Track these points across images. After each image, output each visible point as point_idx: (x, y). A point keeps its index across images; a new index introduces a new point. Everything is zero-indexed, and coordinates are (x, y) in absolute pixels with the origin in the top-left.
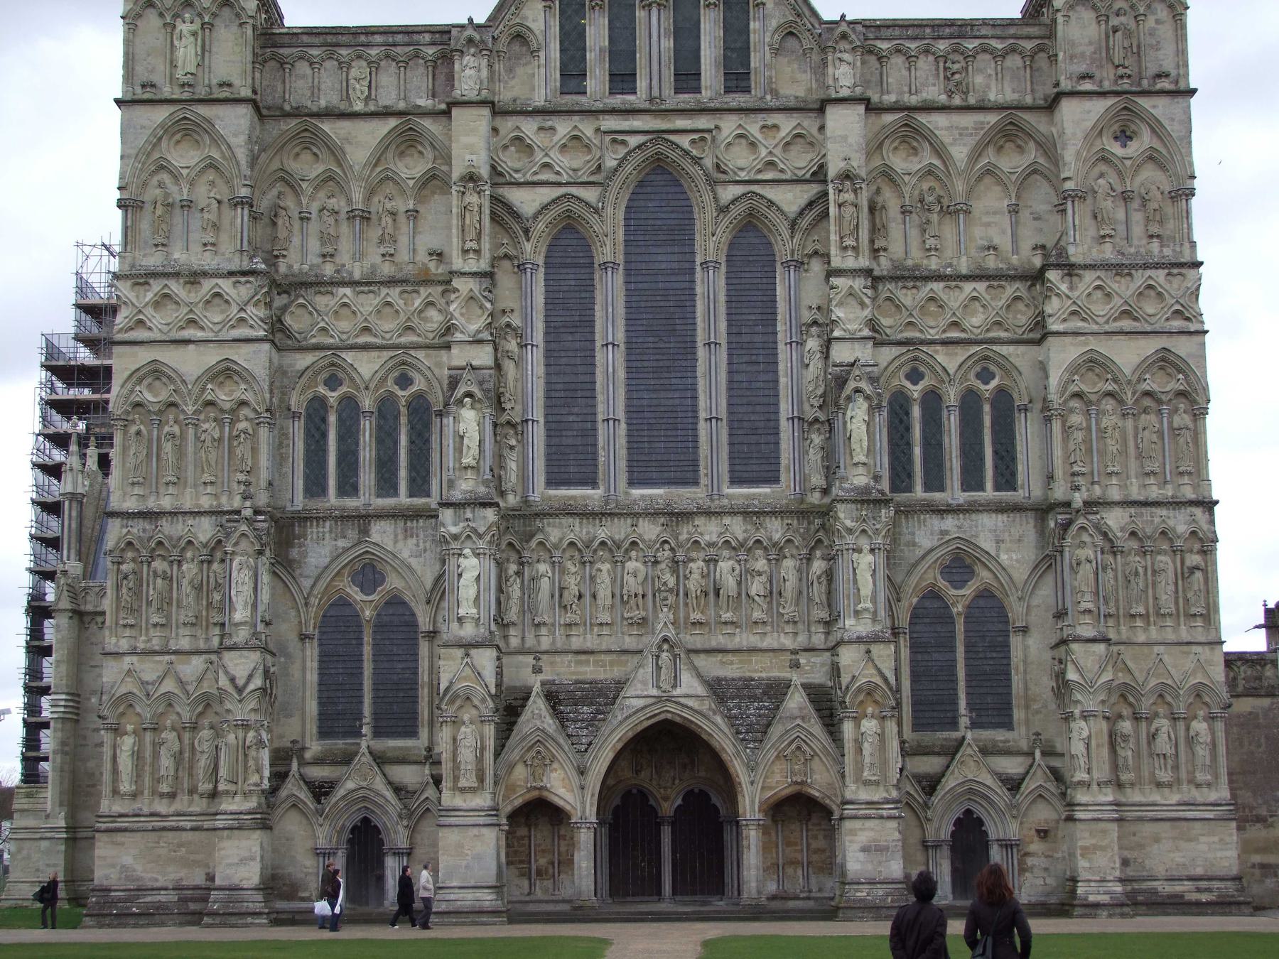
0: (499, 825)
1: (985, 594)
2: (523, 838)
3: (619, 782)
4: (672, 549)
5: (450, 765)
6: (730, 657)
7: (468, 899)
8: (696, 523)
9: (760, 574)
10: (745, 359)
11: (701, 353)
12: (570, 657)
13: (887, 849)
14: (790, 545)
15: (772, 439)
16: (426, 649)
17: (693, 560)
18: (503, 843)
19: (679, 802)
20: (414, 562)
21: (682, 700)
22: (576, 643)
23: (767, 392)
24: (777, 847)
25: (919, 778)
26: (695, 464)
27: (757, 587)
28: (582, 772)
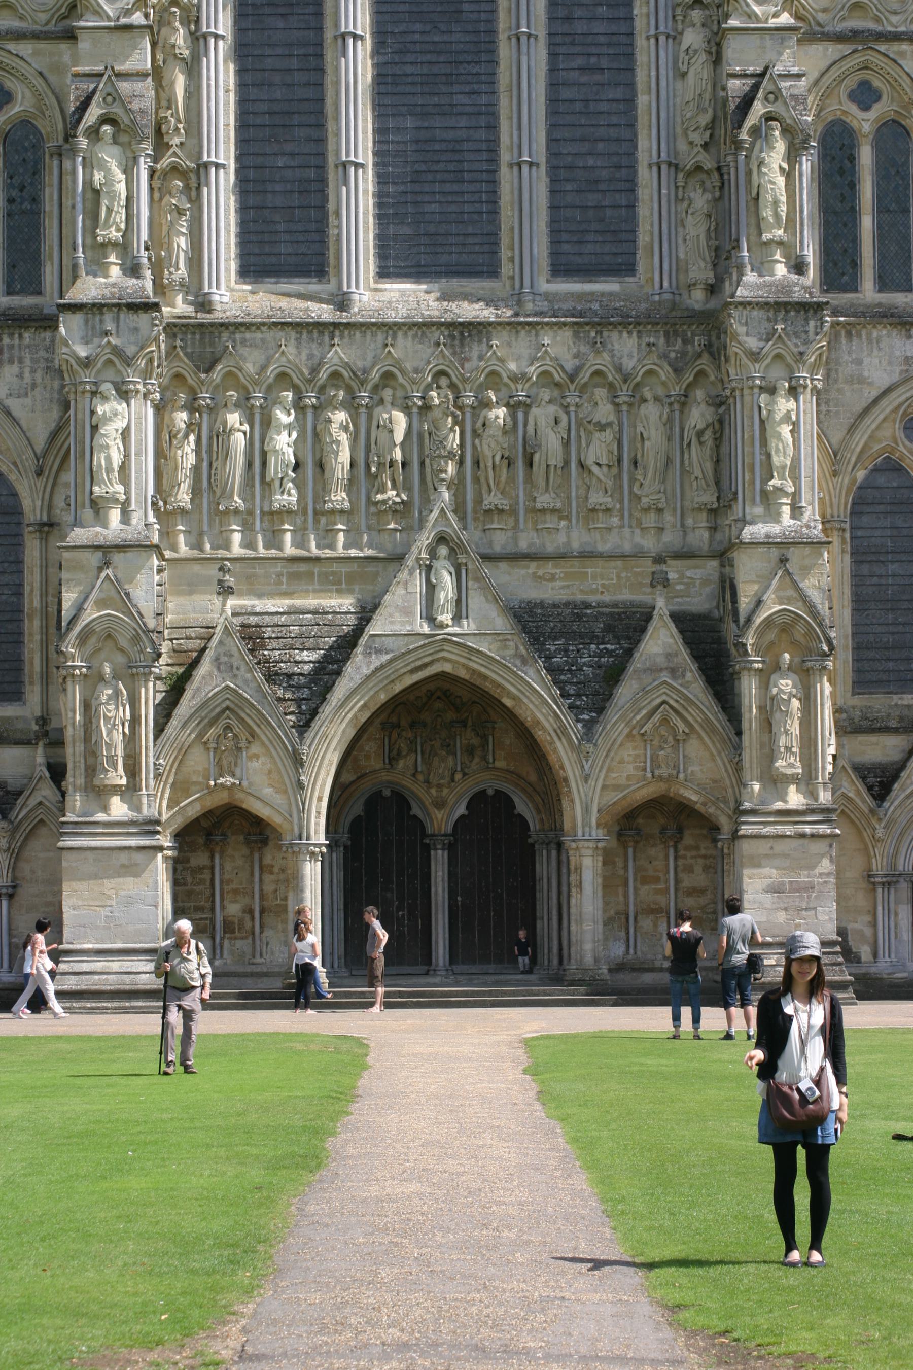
2: (201, 869)
4: (452, 386)
5: (80, 748)
6: (549, 568)
9: (602, 427)
10: (580, 61)
11: (505, 51)
15: (622, 200)
16: (37, 554)
19: (461, 810)
23: (614, 119)
24: (626, 885)
25: (863, 771)
26: (492, 241)
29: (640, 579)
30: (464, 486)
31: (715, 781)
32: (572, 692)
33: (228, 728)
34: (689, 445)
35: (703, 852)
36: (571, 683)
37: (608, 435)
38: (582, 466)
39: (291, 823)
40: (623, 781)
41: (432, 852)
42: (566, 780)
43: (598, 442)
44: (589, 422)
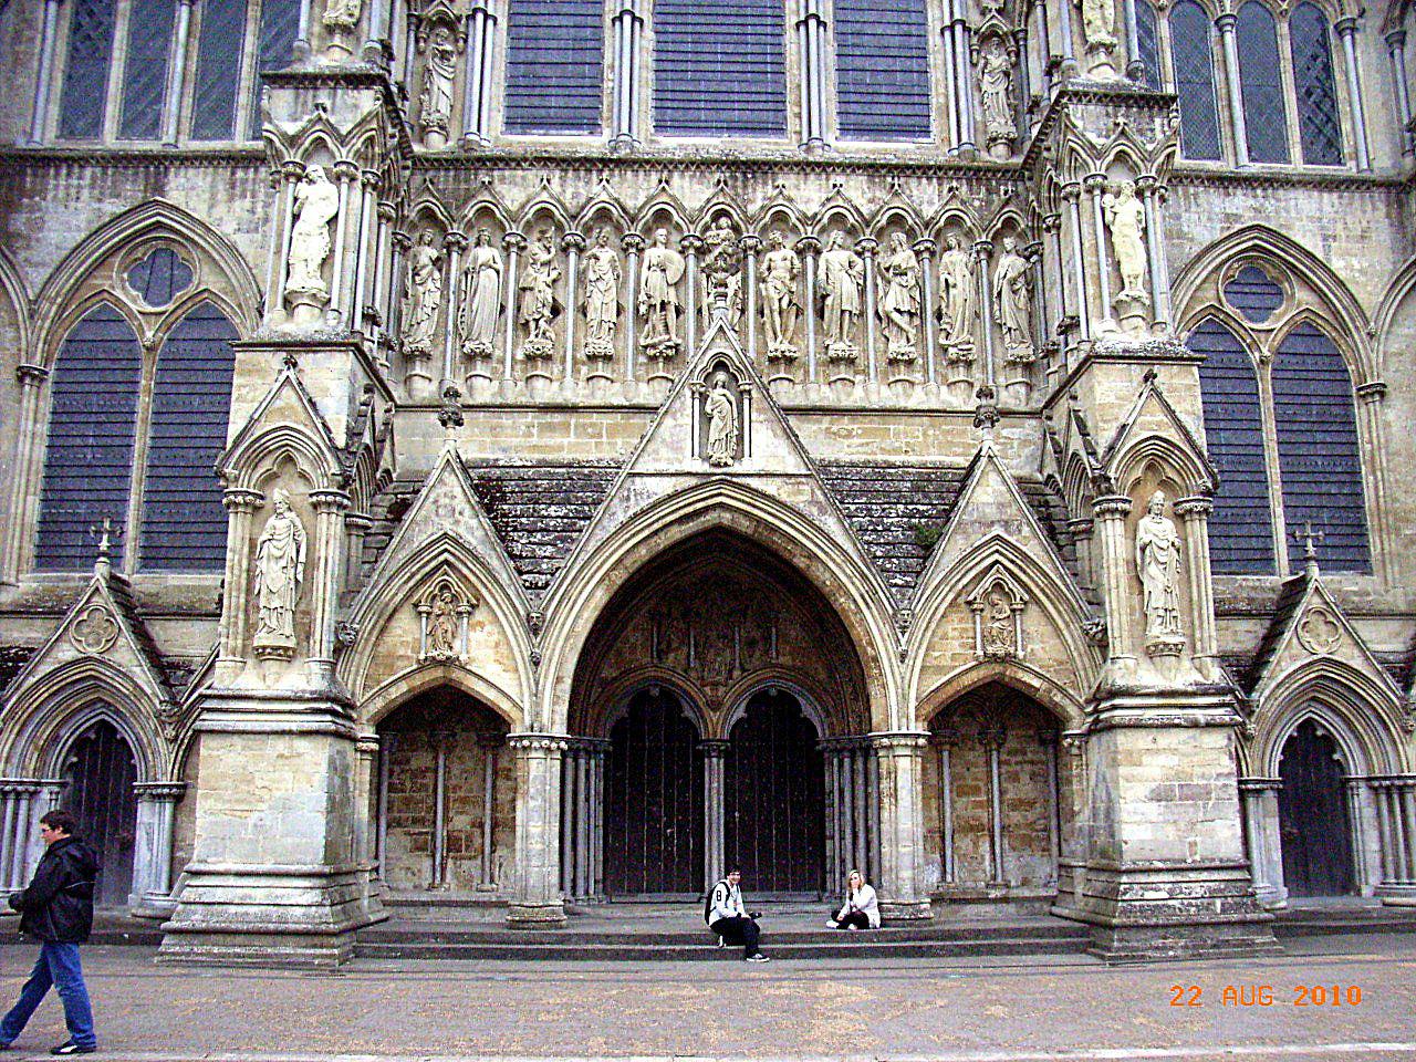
1: (1305, 330)
2: (423, 772)
4: (736, 228)
7: (256, 901)
8: (780, 182)
12: (530, 417)
13: (1207, 792)
14: (956, 230)
17: (773, 247)
18: (362, 774)
19: (740, 713)
20: (242, 242)
21: (754, 483)
22: (544, 392)
24: (941, 796)
26: (779, 99)
27: (895, 298)
28: (535, 629)
30: (746, 335)
32: (879, 554)
34: (999, 294)
36: (877, 544)
37: (910, 279)
38: (880, 319)
39: (522, 710)
40: (946, 662)
41: (706, 760)
42: (875, 659)
43: (899, 288)
44: (887, 269)
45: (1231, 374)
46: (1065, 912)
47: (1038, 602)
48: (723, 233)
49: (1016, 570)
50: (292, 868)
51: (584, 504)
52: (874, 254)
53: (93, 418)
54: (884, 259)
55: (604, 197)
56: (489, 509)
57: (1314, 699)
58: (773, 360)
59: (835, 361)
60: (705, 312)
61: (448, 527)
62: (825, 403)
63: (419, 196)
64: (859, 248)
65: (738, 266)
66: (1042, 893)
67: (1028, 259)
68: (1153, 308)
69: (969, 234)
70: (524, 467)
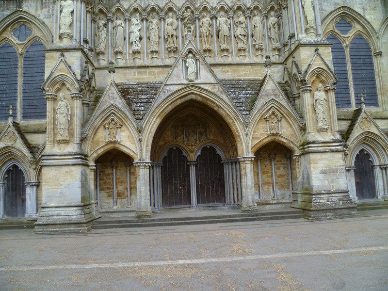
0: (88, 166)
1: (359, 37)
2: (109, 174)
3: (167, 143)
4: (192, 12)
6: (226, 68)
12: (135, 70)
17: (204, 17)
18: (91, 176)
19: (199, 153)
20: (46, 21)
22: (139, 62)
24: (258, 175)
28: (140, 131)
29: (257, 72)
31: (292, 135)
33: (113, 120)
35: (283, 162)
37: (244, 25)
42: (239, 136)
44: (237, 23)
45: (337, 50)
46: (296, 206)
47: (285, 118)
48: (189, 14)
49: (278, 109)
50: (72, 204)
51: (152, 94)
52: (233, 18)
53: (5, 76)
54: (236, 20)
55: (153, 4)
56: (124, 97)
57: (364, 143)
58: (205, 51)
59: (223, 50)
60: (184, 37)
61: (112, 102)
62: (221, 63)
63: (98, 5)
64: (228, 17)
65: (193, 22)
66: (288, 201)
67: (278, 18)
68: (316, 30)
69: (261, 12)
70: (134, 84)
